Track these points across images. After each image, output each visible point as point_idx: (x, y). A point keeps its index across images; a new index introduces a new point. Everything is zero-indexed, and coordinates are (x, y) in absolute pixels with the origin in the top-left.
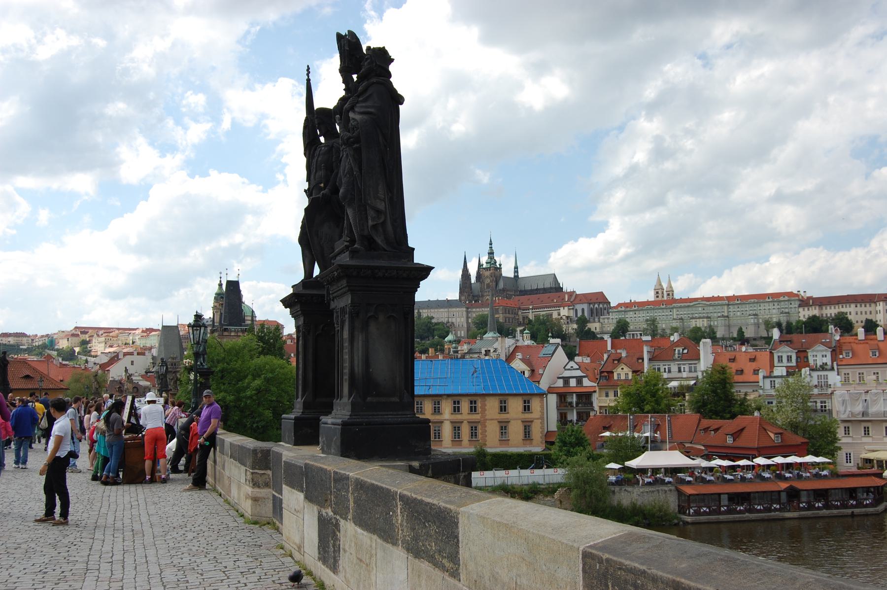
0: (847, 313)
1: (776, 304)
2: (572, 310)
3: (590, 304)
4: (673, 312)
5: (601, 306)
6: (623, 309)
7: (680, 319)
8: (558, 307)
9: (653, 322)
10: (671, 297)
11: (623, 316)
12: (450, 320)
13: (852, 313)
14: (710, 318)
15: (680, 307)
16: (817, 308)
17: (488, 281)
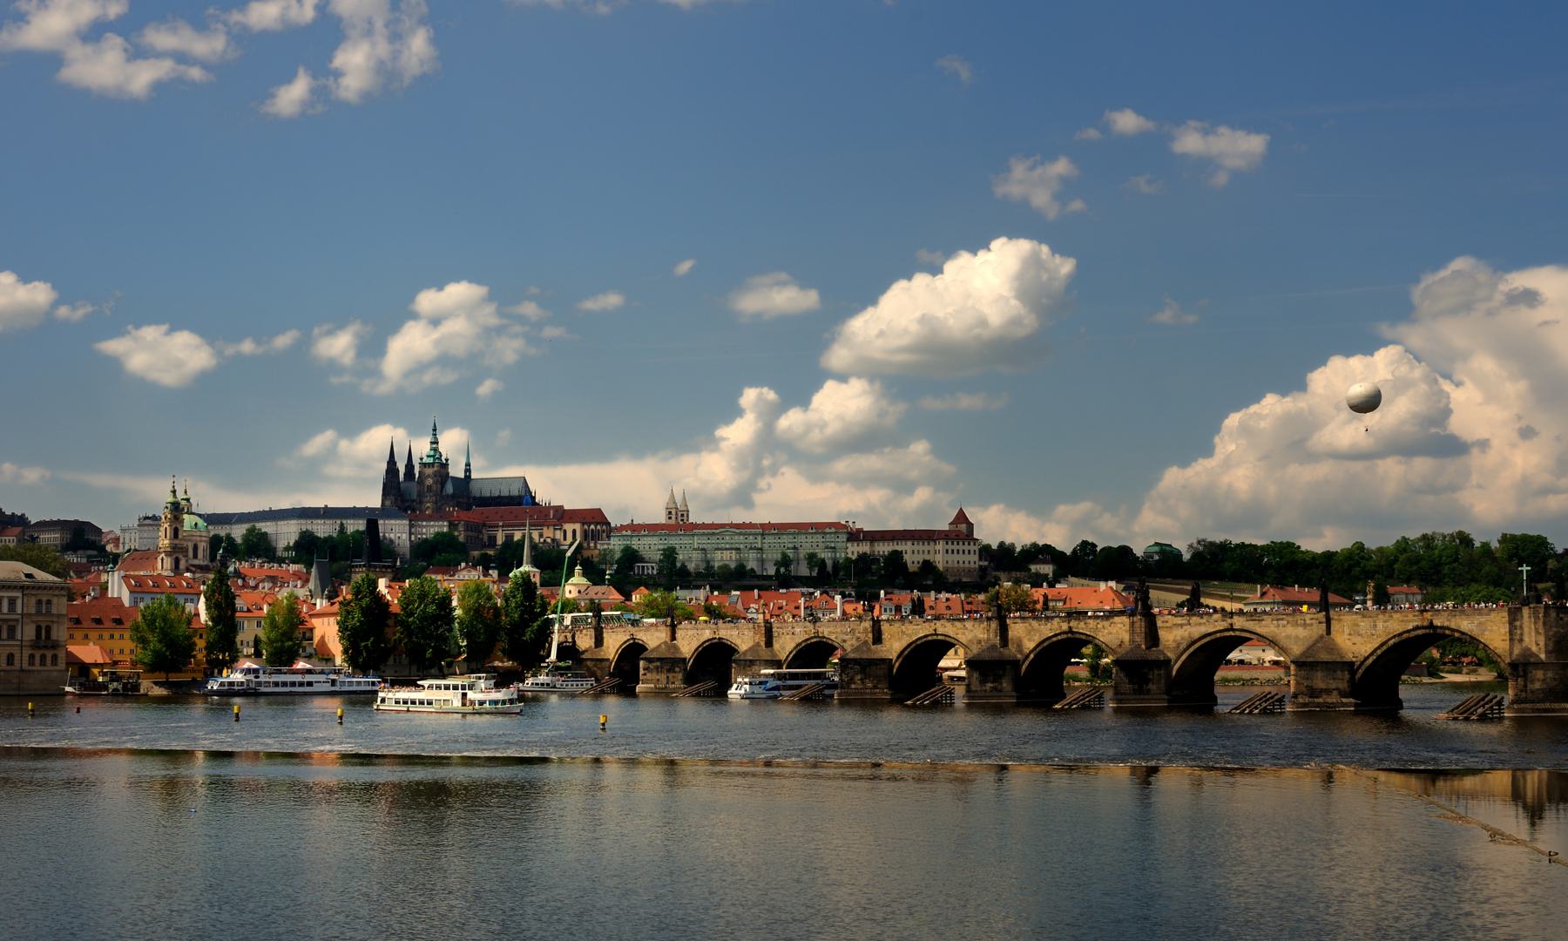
0: (902, 552)
1: (820, 536)
2: (558, 532)
3: (583, 524)
4: (694, 540)
5: (599, 527)
6: (629, 533)
7: (702, 549)
8: (544, 525)
9: (670, 554)
10: (685, 518)
11: (628, 542)
12: (387, 535)
13: (908, 552)
14: (739, 549)
15: (703, 534)
16: (869, 544)
17: (429, 481)
